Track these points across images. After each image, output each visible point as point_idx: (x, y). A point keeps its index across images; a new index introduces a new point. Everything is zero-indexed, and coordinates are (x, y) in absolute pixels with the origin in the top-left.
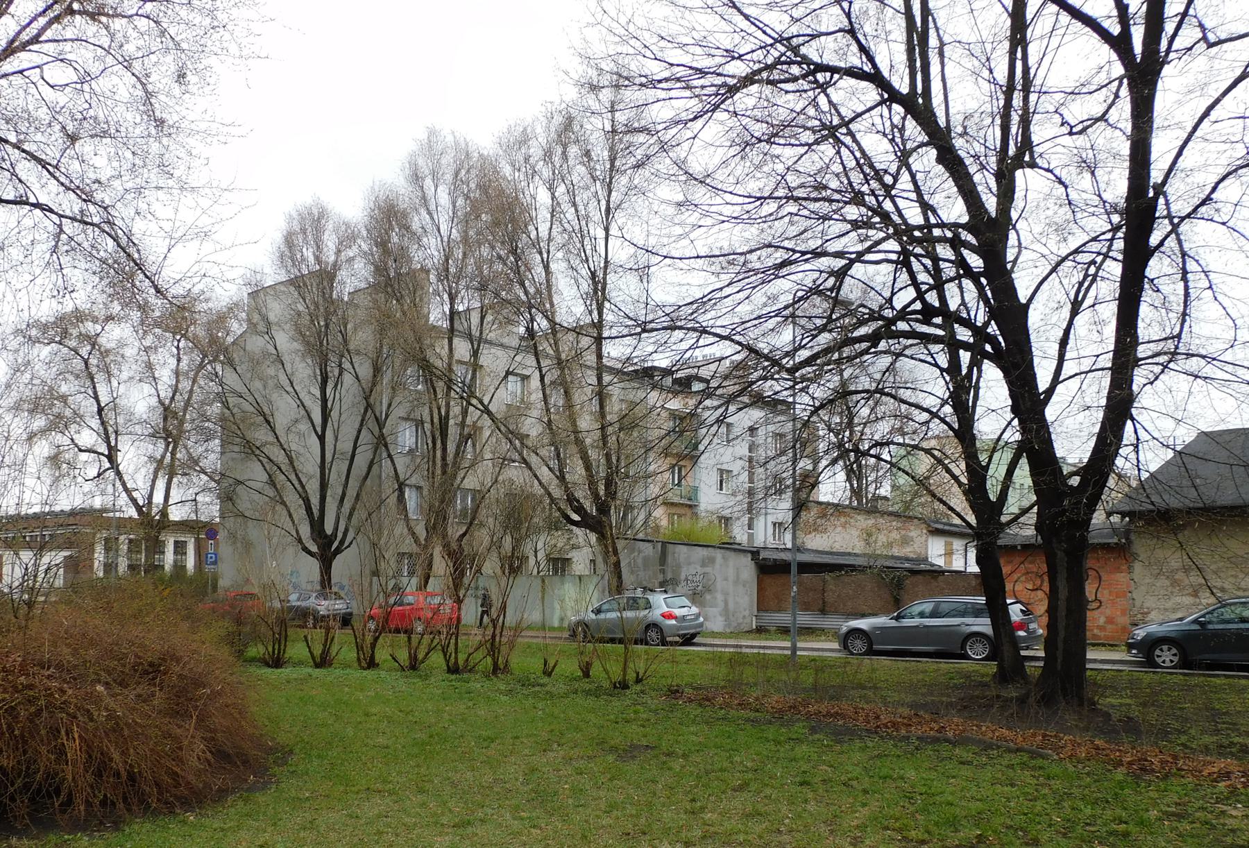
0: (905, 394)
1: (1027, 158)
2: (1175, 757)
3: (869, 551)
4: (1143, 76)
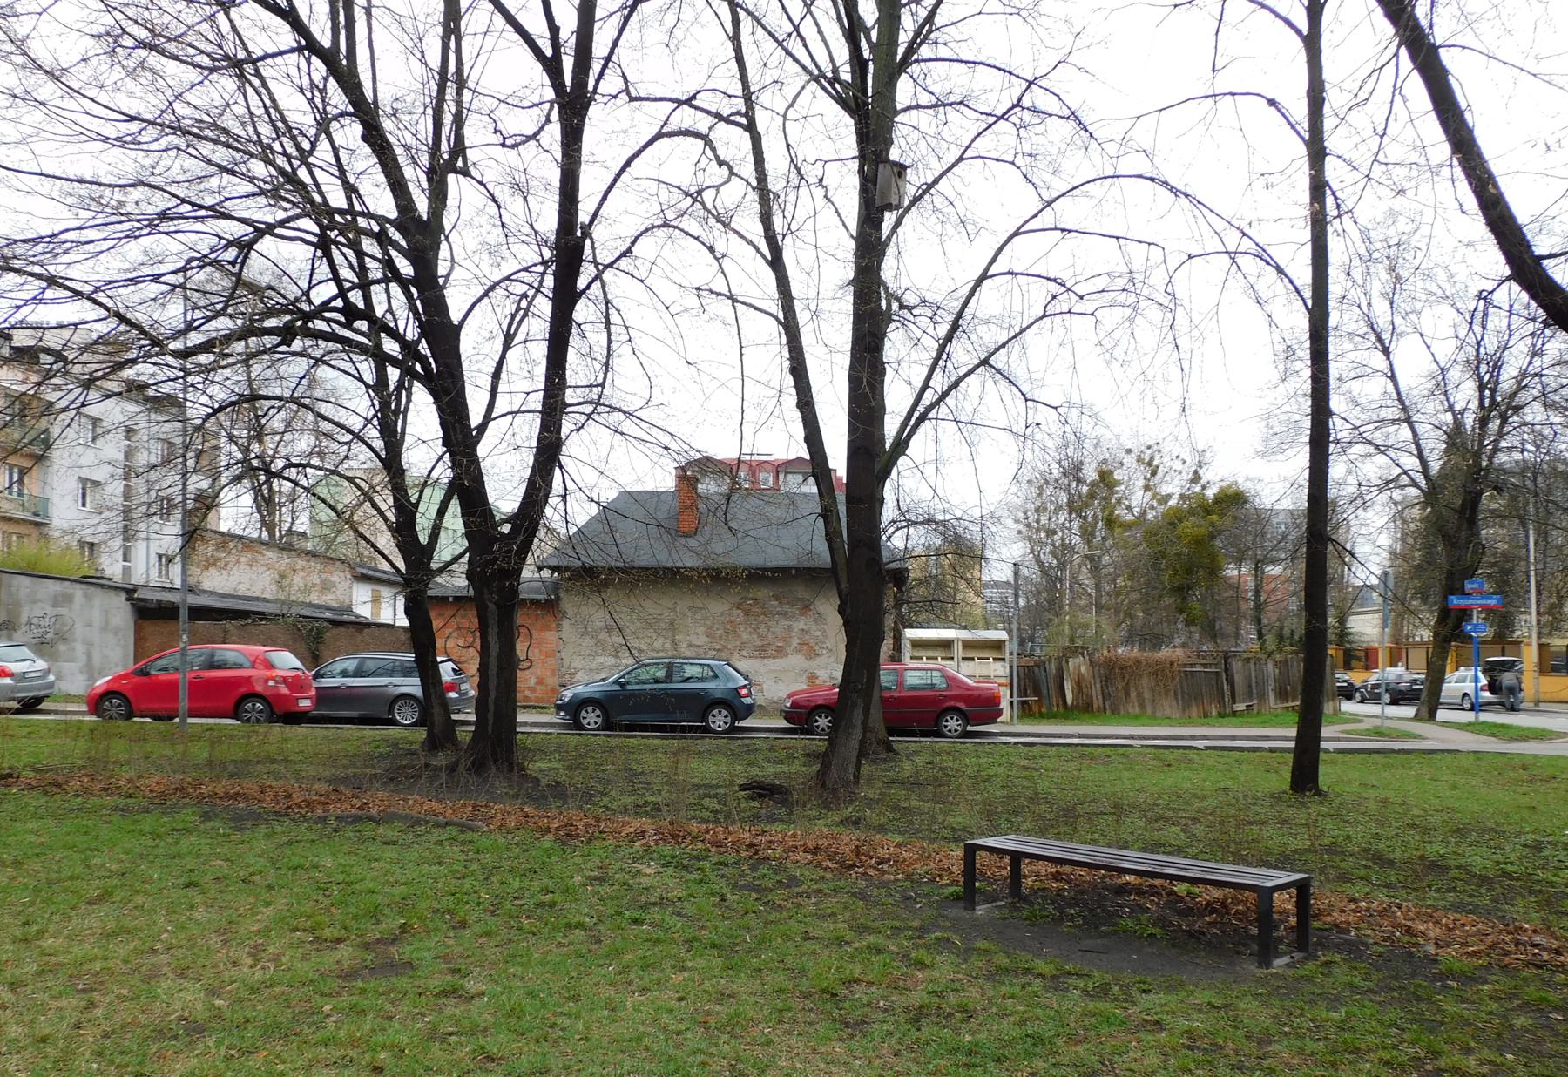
0: (324, 408)
1: (460, 164)
2: (598, 820)
3: (281, 596)
4: (573, 106)
